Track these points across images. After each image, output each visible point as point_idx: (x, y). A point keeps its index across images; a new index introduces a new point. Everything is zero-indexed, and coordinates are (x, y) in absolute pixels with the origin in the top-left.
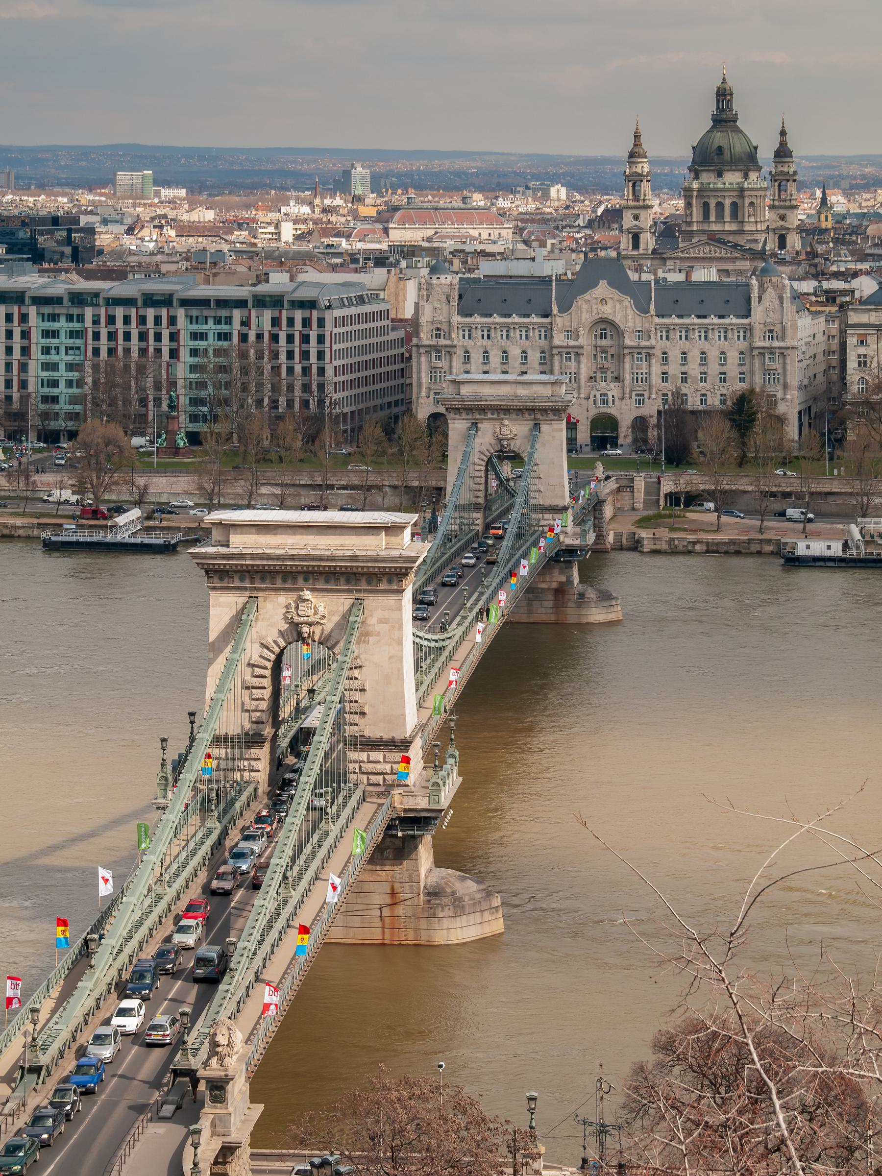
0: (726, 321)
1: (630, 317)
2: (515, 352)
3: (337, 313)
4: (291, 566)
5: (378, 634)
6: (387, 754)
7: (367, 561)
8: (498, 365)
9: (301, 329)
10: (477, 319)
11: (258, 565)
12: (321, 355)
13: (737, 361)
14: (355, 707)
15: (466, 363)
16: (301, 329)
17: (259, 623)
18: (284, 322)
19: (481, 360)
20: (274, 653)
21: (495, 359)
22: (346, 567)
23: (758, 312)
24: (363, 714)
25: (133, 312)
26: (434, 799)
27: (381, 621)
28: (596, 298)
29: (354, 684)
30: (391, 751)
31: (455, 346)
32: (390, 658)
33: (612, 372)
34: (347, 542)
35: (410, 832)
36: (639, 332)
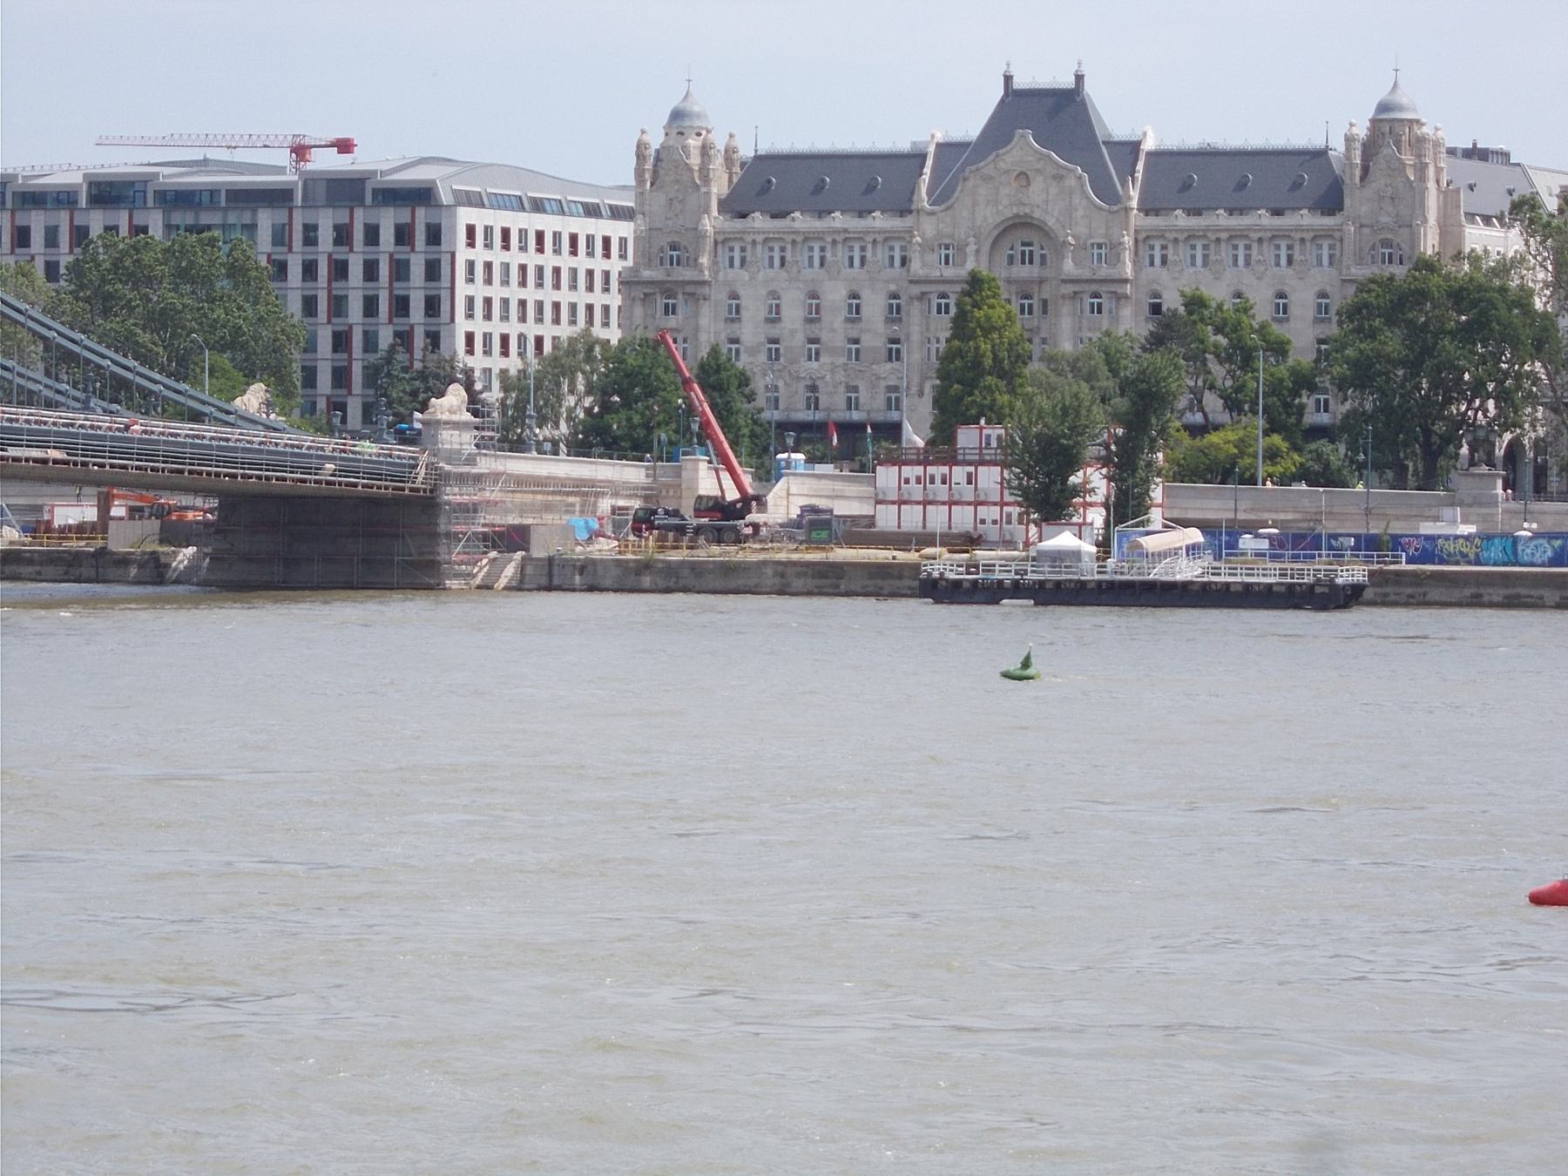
0: (1287, 221)
1: (1080, 213)
2: (835, 295)
3: (466, 216)
8: (799, 325)
9: (391, 248)
10: (759, 221)
12: (432, 306)
13: (1310, 313)
15: (732, 320)
16: (391, 248)
18: (359, 235)
19: (763, 313)
21: (793, 314)
23: (1357, 202)
25: (63, 219)
28: (1007, 172)
31: (704, 283)
33: (1044, 341)
36: (1100, 246)
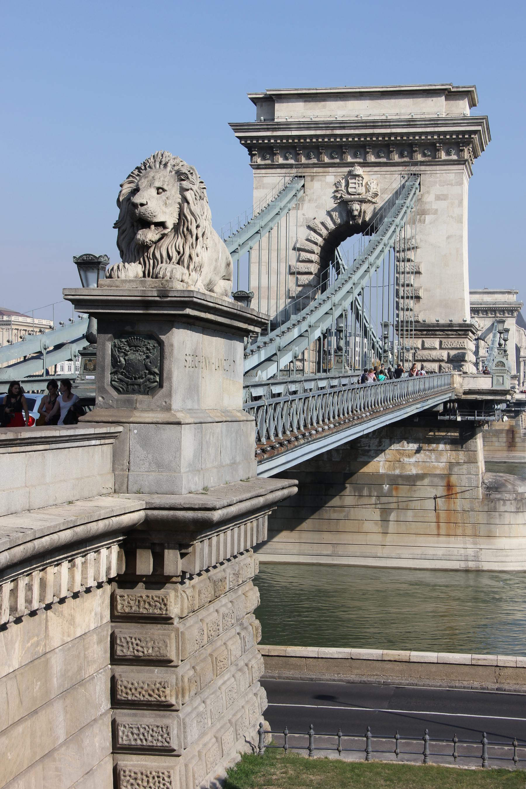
4: (341, 136)
5: (436, 212)
6: (444, 340)
7: (426, 126)
11: (305, 137)
14: (409, 291)
17: (306, 205)
20: (321, 235)
22: (402, 135)
24: (418, 298)
26: (498, 380)
27: (438, 198)
29: (408, 267)
30: (448, 336)
32: (448, 238)
34: (403, 111)
35: (469, 418)
